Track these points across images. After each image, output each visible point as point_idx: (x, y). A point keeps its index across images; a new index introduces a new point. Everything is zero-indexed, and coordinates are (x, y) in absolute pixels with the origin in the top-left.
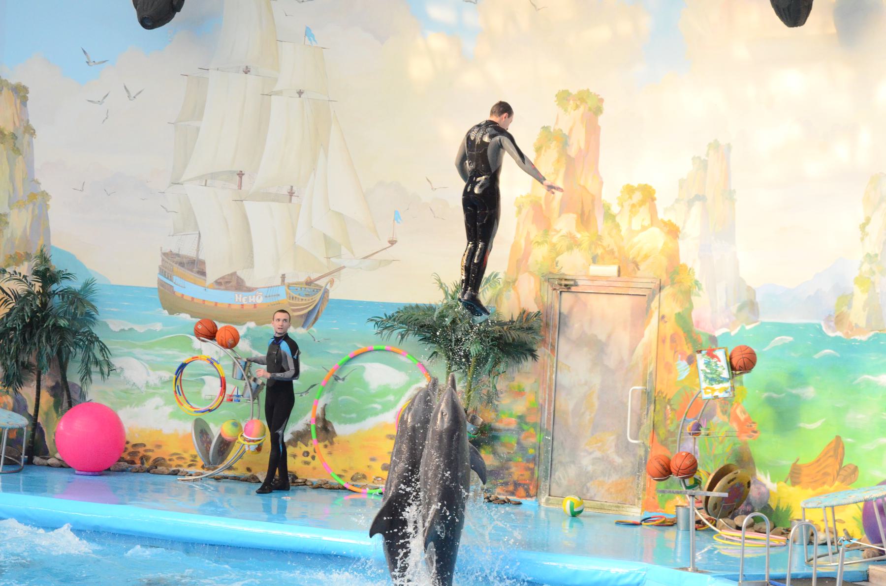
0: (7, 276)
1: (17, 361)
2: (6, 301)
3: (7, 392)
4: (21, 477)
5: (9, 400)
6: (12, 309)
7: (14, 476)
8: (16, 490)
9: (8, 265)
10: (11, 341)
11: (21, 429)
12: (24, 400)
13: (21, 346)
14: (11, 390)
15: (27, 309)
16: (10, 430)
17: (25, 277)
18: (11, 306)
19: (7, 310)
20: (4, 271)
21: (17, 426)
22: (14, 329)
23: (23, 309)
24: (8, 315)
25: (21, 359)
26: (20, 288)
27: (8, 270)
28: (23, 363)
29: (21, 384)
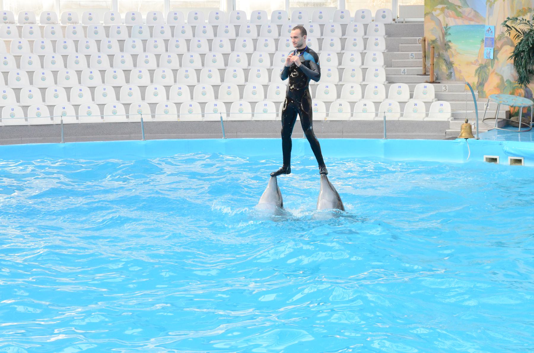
0: (518, 21)
1: (526, 69)
2: (518, 36)
3: (521, 87)
4: (531, 134)
5: (522, 91)
6: (522, 40)
7: (527, 133)
8: (529, 140)
9: (519, 16)
10: (522, 58)
11: (529, 107)
12: (531, 92)
13: (528, 61)
14: (523, 86)
15: (530, 39)
16: (524, 108)
17: (528, 21)
18: (521, 38)
19: (519, 41)
20: (517, 19)
21: (527, 105)
22: (523, 51)
23: (528, 40)
24: (520, 43)
25: (528, 68)
26: (526, 28)
27: (518, 18)
28: (529, 70)
29: (529, 82)
